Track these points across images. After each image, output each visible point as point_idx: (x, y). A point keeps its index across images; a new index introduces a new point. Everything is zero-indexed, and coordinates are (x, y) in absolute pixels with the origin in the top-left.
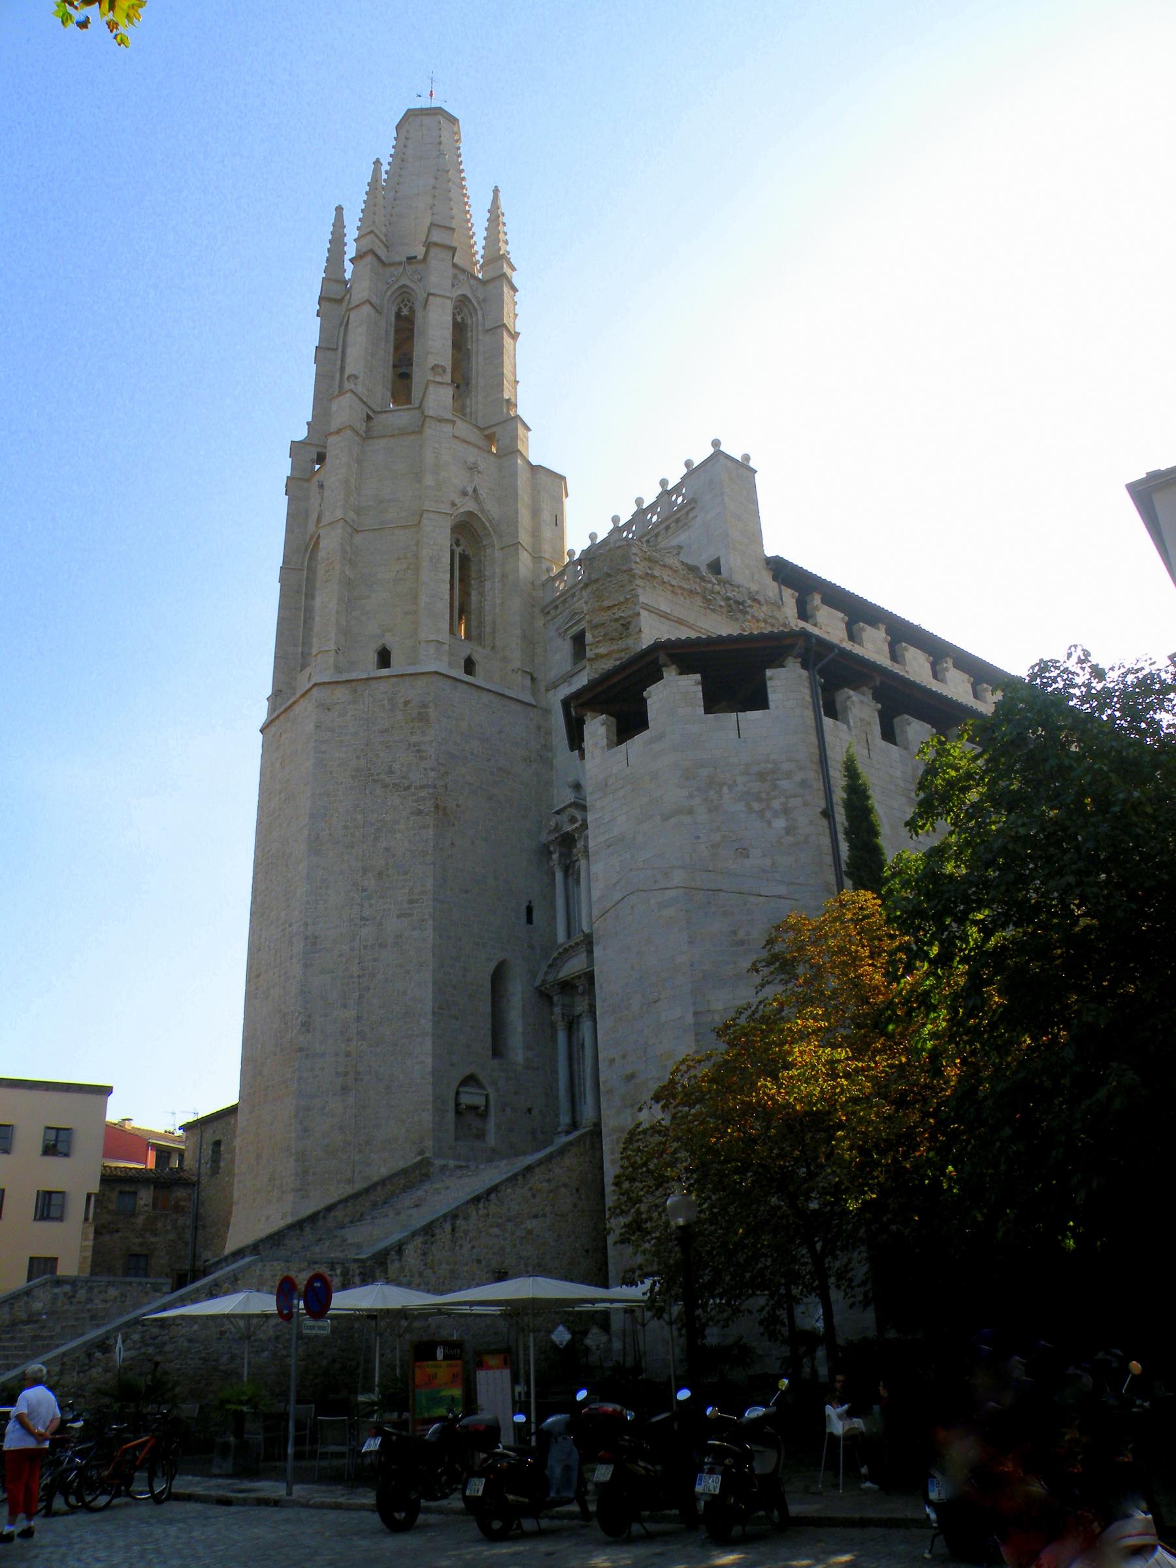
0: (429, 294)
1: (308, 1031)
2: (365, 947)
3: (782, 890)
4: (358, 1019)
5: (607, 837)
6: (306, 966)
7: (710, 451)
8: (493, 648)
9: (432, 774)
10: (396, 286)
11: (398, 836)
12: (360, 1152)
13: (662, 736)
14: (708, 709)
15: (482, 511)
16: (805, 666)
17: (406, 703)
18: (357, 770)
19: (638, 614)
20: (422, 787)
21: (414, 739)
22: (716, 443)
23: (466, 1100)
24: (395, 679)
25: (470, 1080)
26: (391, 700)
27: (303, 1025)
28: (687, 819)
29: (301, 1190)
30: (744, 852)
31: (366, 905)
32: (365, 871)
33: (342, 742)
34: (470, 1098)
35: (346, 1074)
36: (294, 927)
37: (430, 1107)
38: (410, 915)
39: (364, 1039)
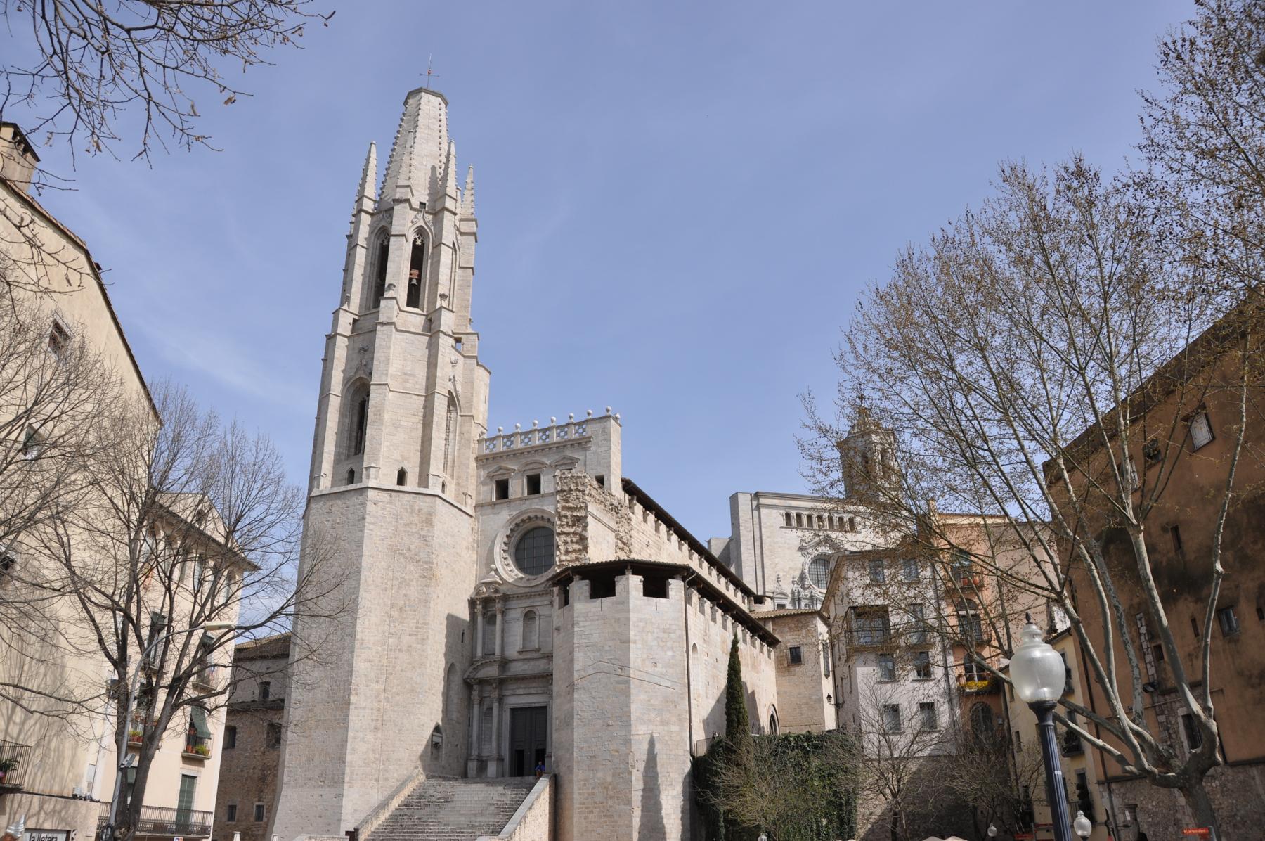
3: (669, 684)
13: (623, 603)
14: (646, 594)
16: (684, 580)
19: (586, 517)
21: (423, 533)
30: (655, 664)
32: (392, 606)
34: (436, 739)
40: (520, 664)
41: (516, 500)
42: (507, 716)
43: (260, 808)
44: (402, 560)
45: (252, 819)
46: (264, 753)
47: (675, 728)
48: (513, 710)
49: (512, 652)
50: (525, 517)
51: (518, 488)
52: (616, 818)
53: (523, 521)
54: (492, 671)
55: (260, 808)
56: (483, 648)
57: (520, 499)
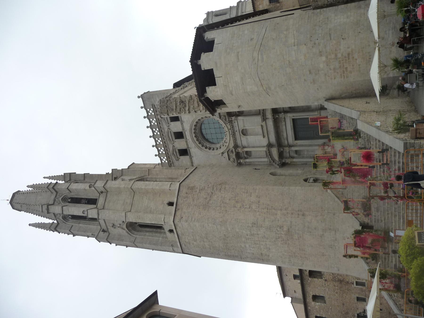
0: (67, 188)
1: (283, 227)
2: (259, 207)
3: (264, 30)
4: (281, 210)
5: (240, 85)
6: (261, 227)
7: (141, 99)
8: (176, 179)
9: (210, 186)
10: (61, 201)
11: (226, 196)
12: (325, 211)
13: (216, 63)
15: (136, 179)
17: (187, 193)
18: (203, 209)
20: (213, 189)
21: (198, 191)
22: (139, 97)
23: (311, 180)
24: (179, 197)
25: (306, 180)
26: (184, 198)
27: (280, 228)
28: (240, 53)
29: (336, 231)
30: (252, 39)
31: (245, 207)
32: (235, 207)
33: (193, 213)
35: (298, 214)
36: (249, 233)
37: (312, 188)
38: (251, 193)
39: (288, 208)
40: (270, 136)
41: (187, 145)
42: (299, 142)
43: (357, 284)
44: (211, 202)
45: (364, 288)
46: (326, 280)
47: (291, 22)
48: (296, 139)
49: (265, 142)
50: (195, 139)
51: (180, 144)
52: (350, 50)
53: (197, 140)
54: (275, 152)
55: (357, 284)
56: (264, 158)
57: (186, 142)
